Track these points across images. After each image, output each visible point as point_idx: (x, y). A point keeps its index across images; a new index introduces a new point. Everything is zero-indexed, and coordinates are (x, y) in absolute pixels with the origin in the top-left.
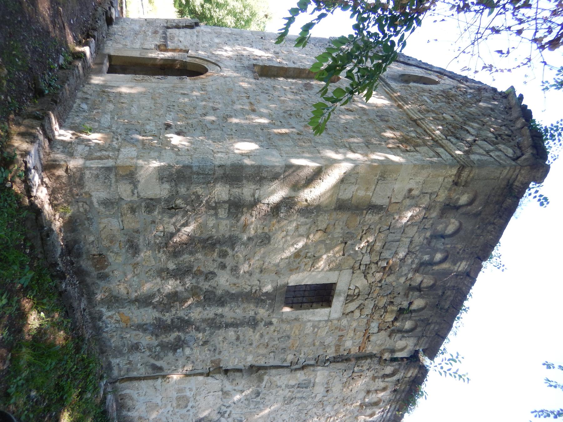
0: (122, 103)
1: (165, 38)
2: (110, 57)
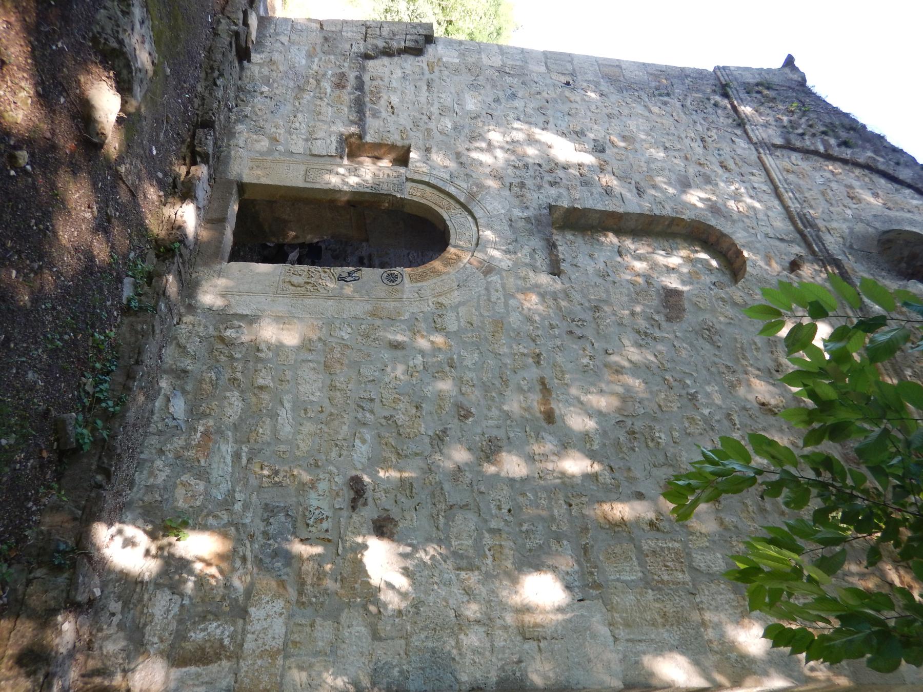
0: (261, 388)
1: (359, 106)
2: (242, 187)
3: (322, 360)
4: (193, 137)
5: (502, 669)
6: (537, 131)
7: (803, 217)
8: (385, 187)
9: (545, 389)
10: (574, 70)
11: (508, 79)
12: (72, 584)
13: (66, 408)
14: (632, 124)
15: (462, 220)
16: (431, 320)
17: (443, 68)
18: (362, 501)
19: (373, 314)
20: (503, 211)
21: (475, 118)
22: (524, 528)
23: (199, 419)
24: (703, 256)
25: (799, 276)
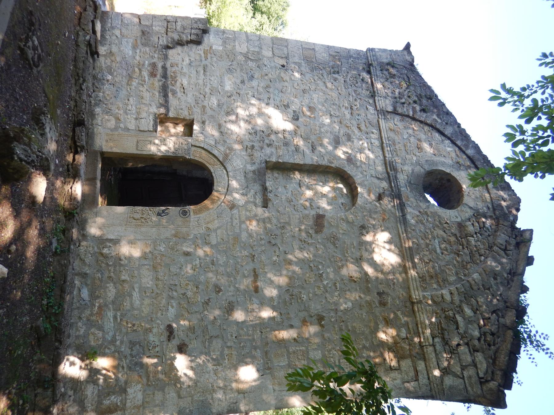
0: (124, 281)
1: (165, 91)
2: (102, 153)
3: (152, 264)
4: (74, 131)
5: (229, 406)
6: (263, 105)
7: (391, 163)
8: (180, 152)
9: (256, 276)
10: (288, 54)
11: (250, 63)
12: (54, 392)
13: (38, 318)
14: (315, 96)
15: (220, 172)
16: (204, 238)
18: (172, 336)
19: (175, 236)
20: (242, 166)
21: (230, 96)
22: (241, 345)
23: (96, 299)
24: (341, 186)
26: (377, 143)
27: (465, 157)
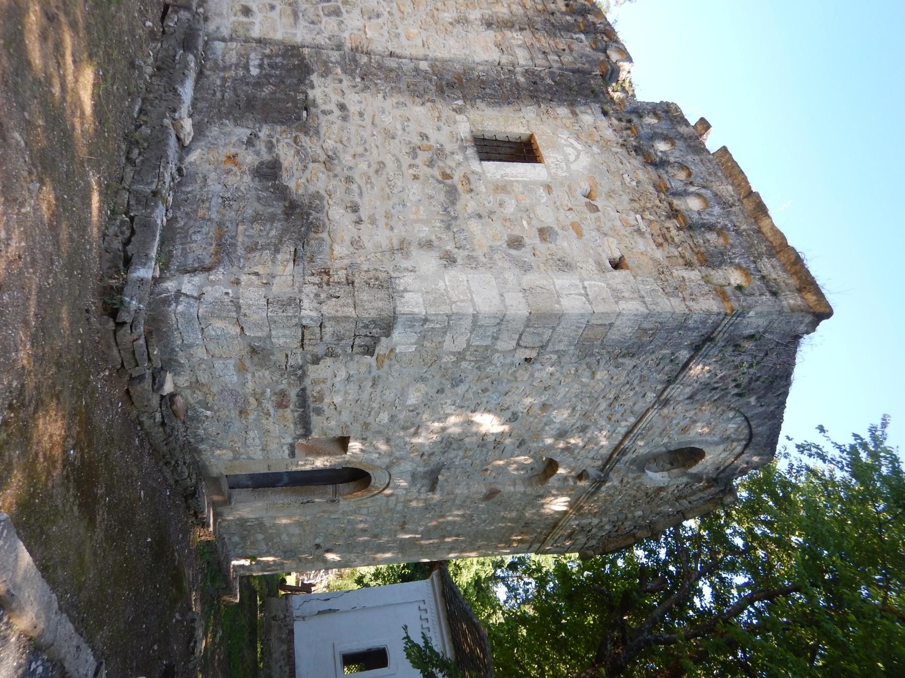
17: (394, 362)
25: (575, 483)
26: (622, 430)
27: (746, 431)
